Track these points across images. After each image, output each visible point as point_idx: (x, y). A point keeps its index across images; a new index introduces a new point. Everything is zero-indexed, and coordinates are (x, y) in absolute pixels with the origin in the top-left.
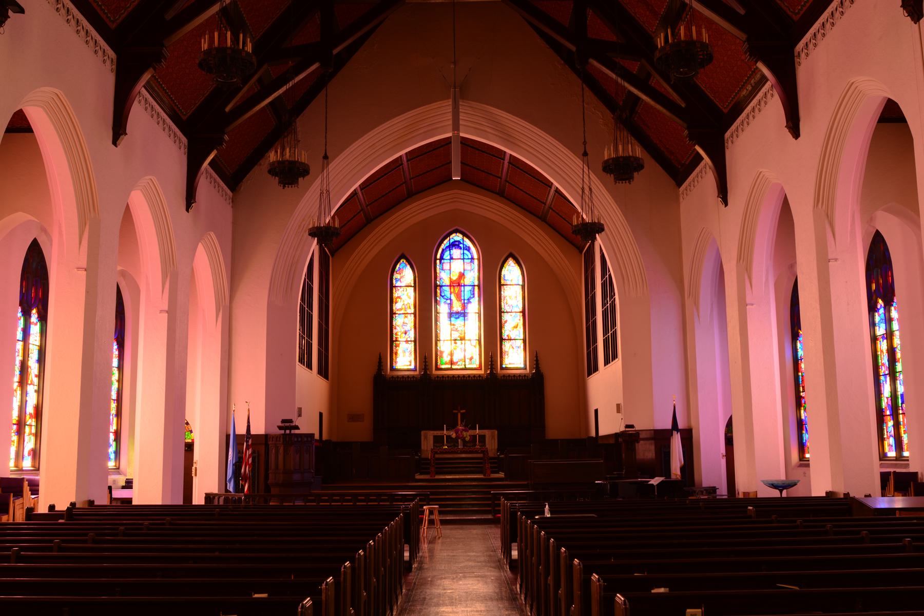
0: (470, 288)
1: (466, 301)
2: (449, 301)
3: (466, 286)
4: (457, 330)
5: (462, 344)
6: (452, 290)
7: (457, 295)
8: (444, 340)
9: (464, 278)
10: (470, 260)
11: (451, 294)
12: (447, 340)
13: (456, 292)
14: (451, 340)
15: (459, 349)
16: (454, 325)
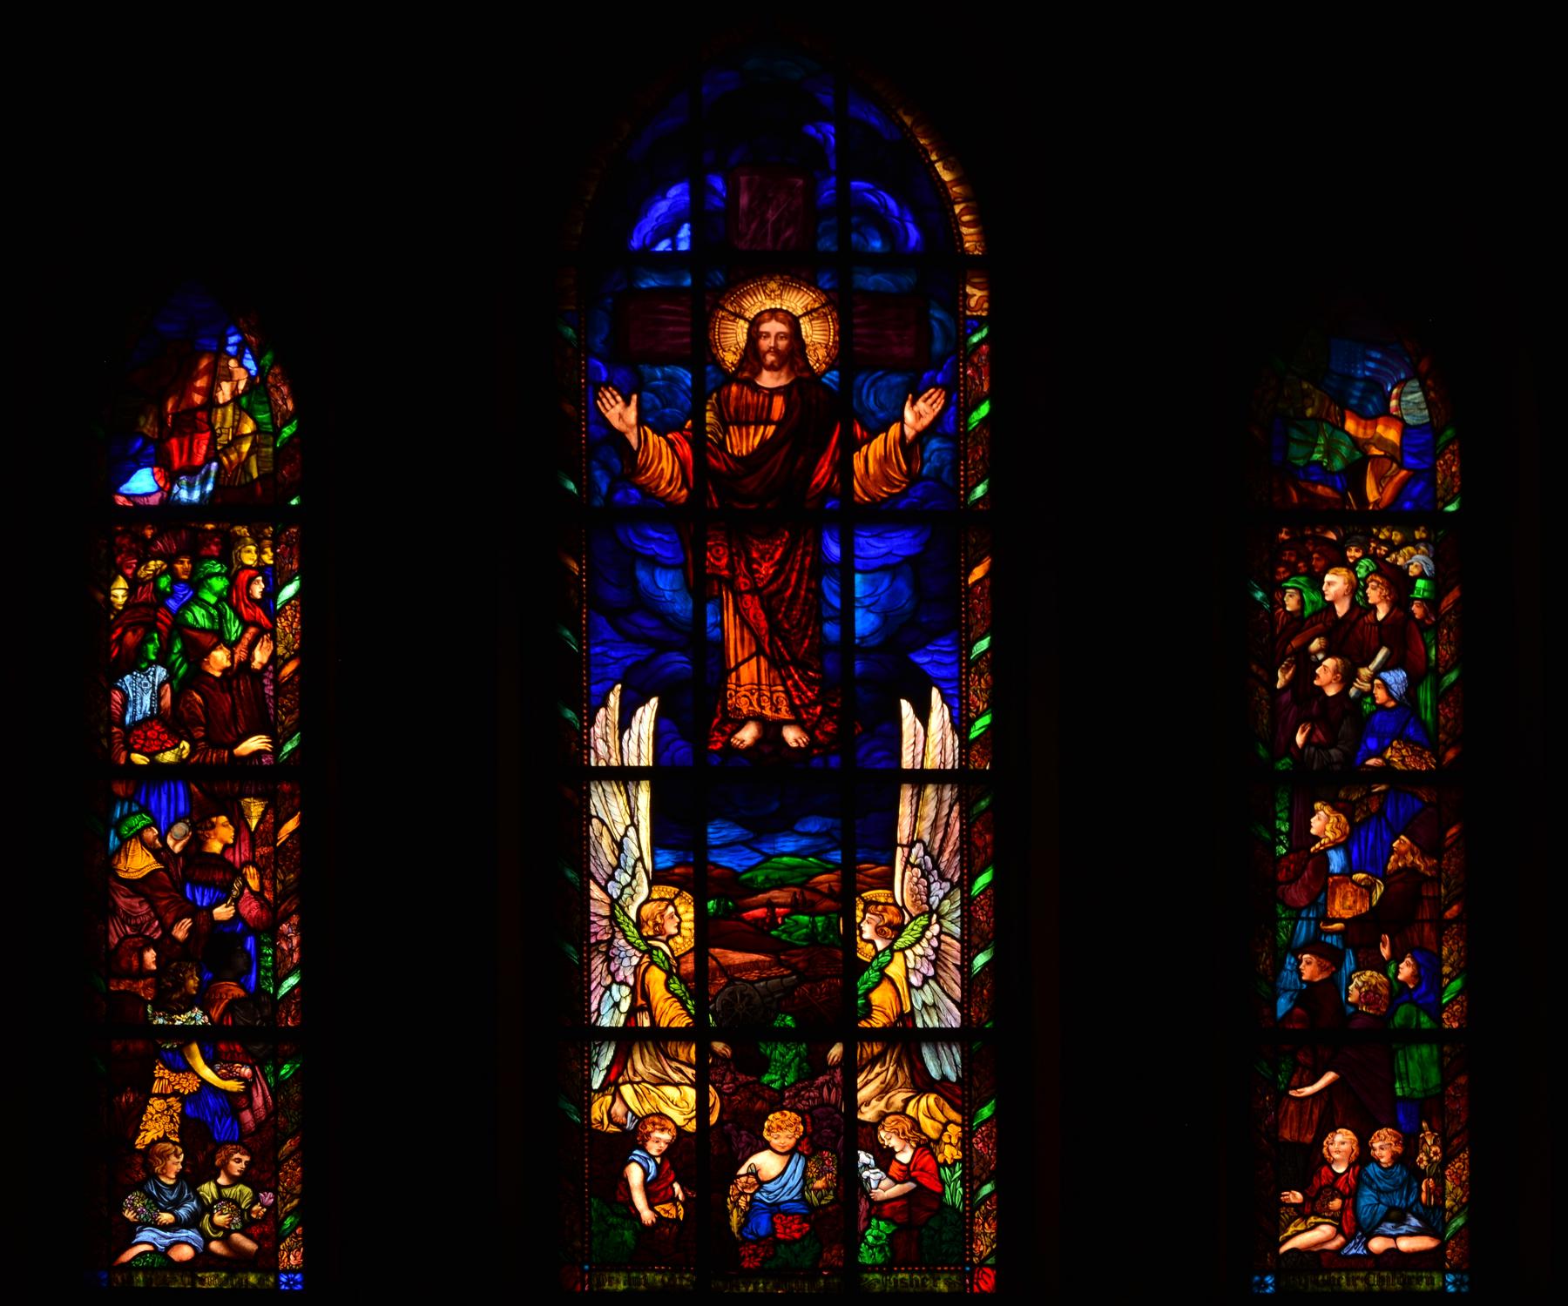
0: (897, 544)
1: (858, 666)
2: (678, 662)
3: (880, 515)
4: (756, 937)
5: (815, 1064)
6: (718, 558)
7: (770, 613)
8: (627, 1038)
9: (851, 445)
10: (908, 280)
11: (702, 589)
12: (661, 1039)
13: (766, 570)
14: (695, 1034)
15: (782, 1129)
16: (735, 888)
